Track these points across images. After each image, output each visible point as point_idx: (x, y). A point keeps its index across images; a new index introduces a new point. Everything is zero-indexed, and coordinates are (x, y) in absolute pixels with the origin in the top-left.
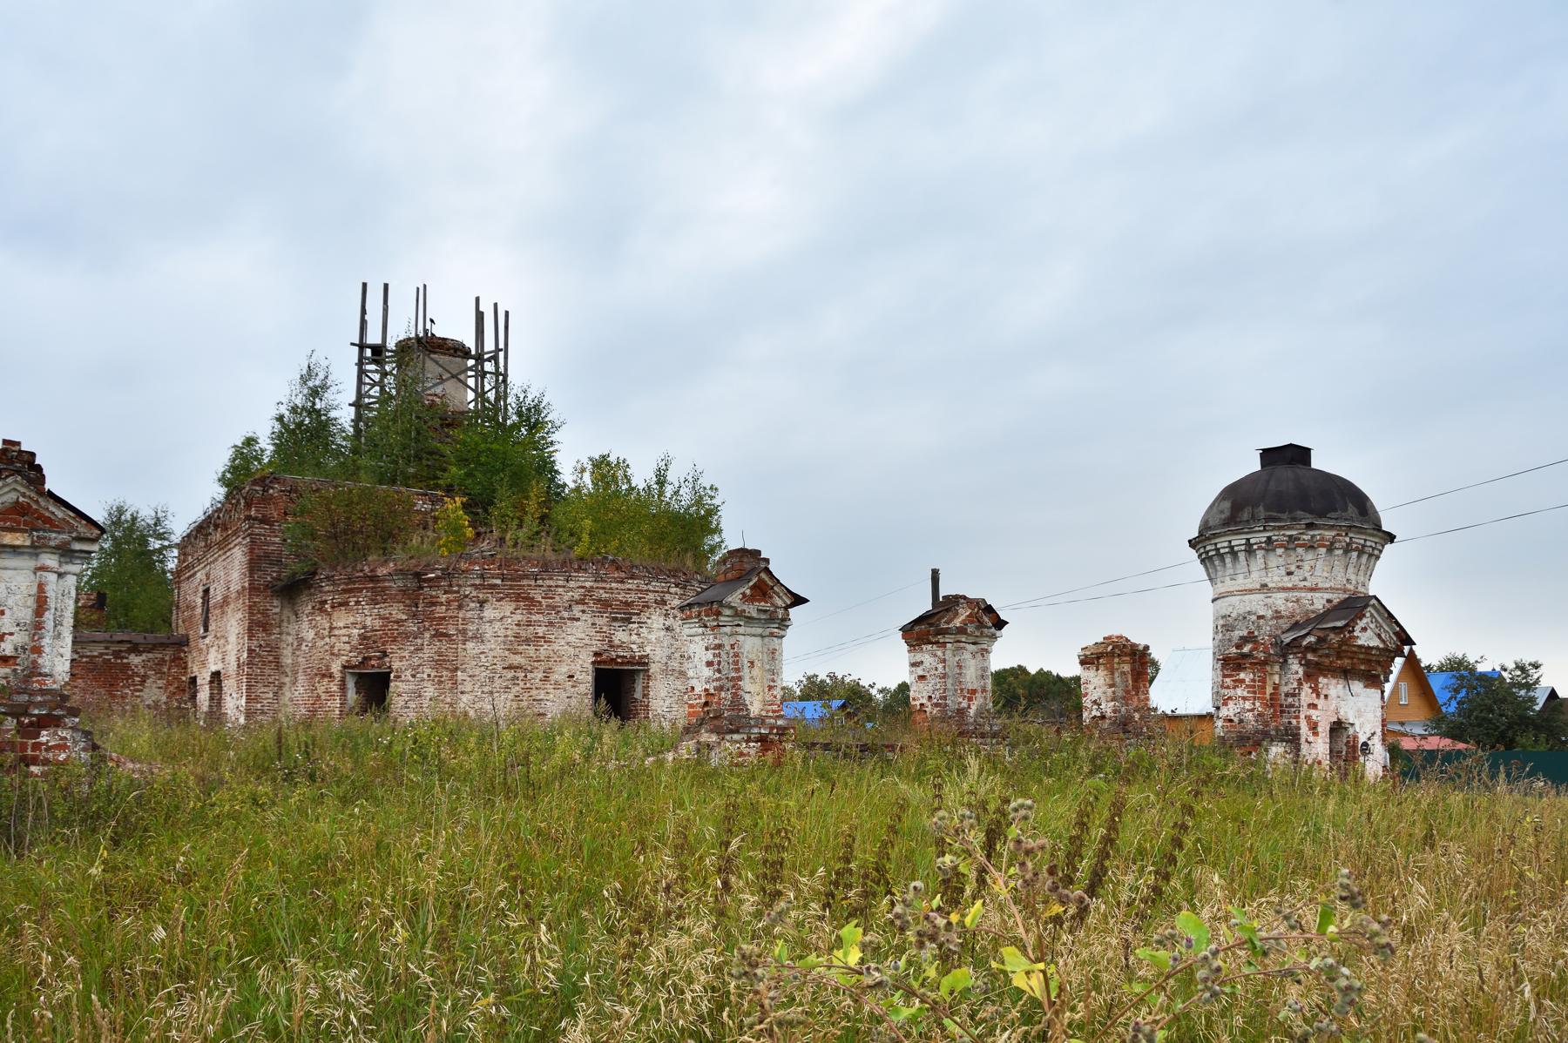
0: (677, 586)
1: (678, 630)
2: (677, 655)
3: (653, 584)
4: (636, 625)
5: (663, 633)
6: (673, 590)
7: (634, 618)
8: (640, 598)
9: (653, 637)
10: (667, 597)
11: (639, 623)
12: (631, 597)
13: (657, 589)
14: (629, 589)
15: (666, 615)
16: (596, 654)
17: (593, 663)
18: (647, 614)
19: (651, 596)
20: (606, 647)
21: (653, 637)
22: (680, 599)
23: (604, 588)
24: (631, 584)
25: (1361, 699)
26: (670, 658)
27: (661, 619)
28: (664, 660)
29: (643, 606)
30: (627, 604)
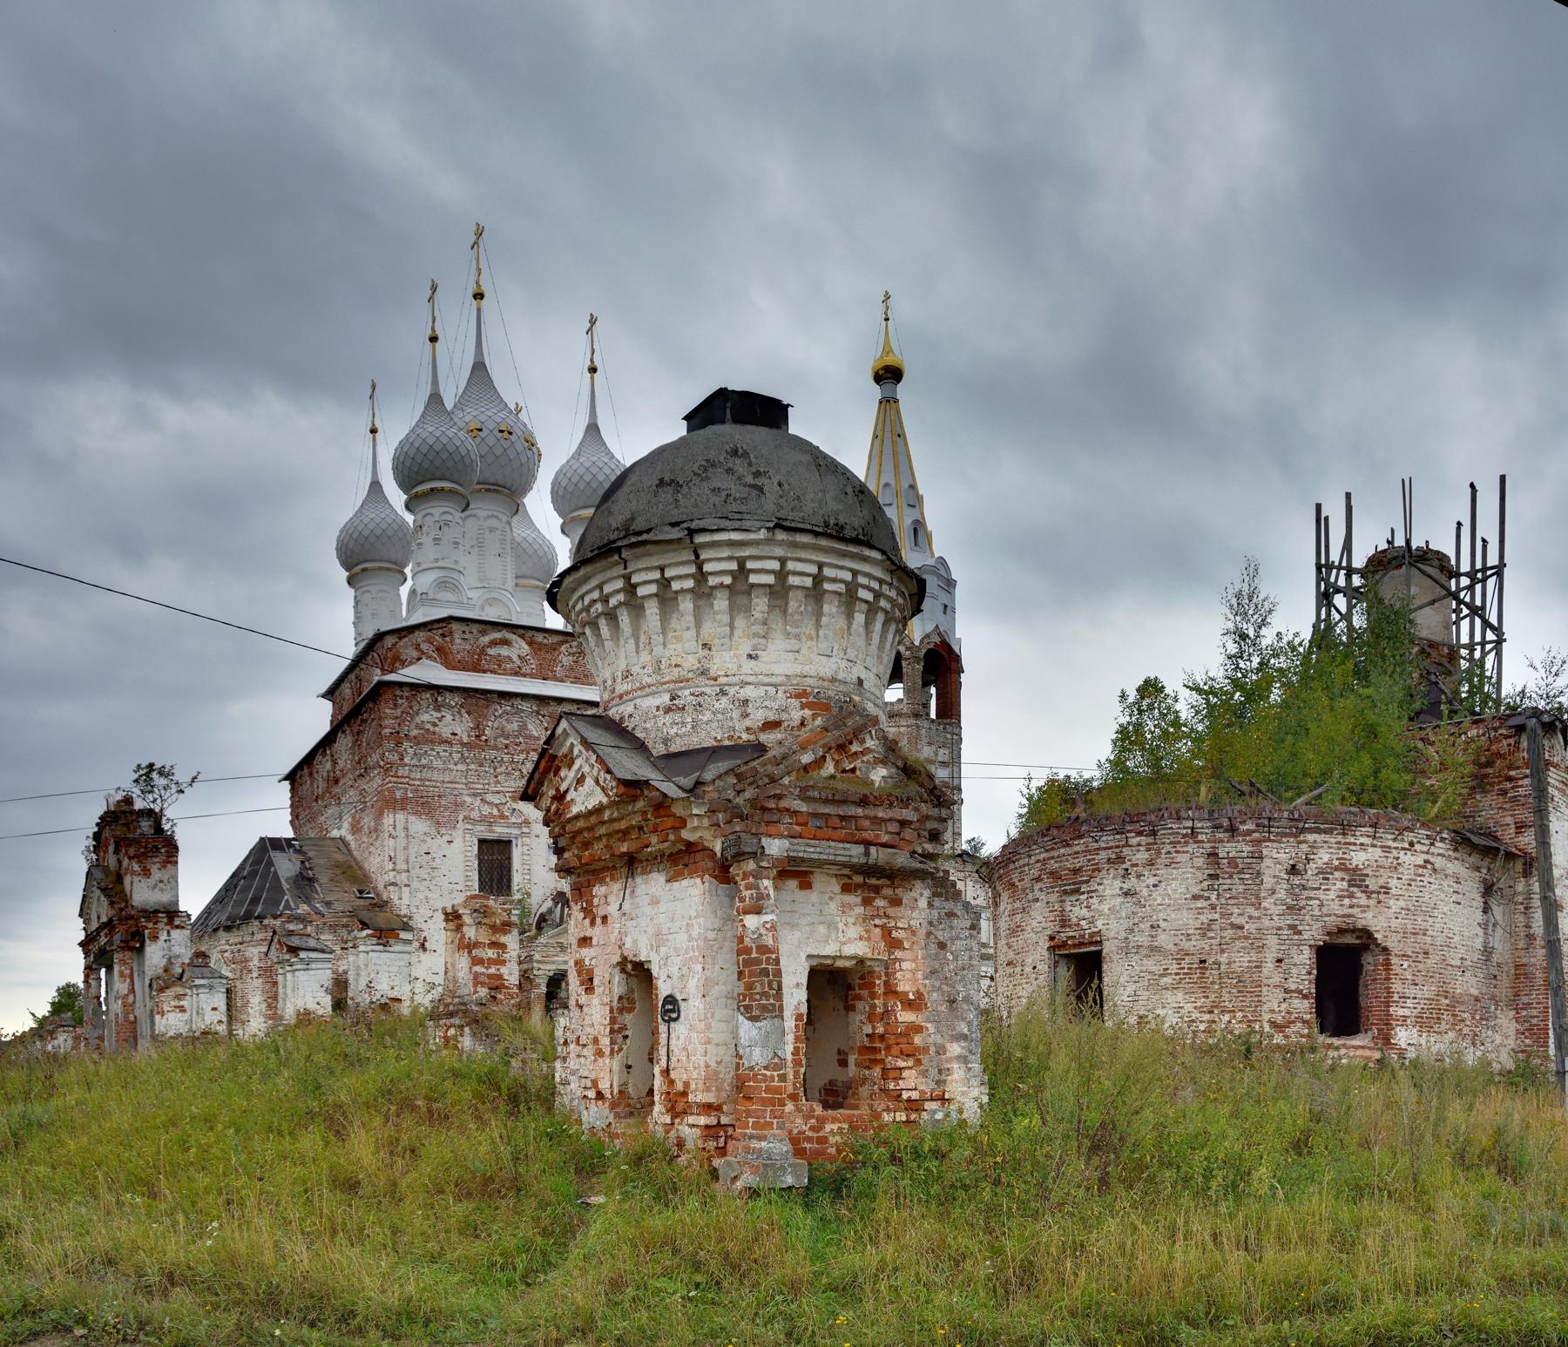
0: (1140, 834)
1: (1145, 892)
2: (1145, 926)
3: (1104, 838)
4: (1086, 896)
5: (1120, 900)
6: (1134, 841)
7: (1084, 888)
8: (1089, 861)
9: (1105, 907)
10: (1126, 851)
11: (1088, 892)
12: (1080, 862)
13: (1111, 844)
14: (1076, 853)
15: (1126, 874)
16: (1052, 938)
17: (1049, 949)
18: (1098, 880)
19: (1103, 855)
20: (1057, 929)
21: (1105, 907)
22: (1148, 850)
23: (1053, 858)
24: (1079, 846)
25: (662, 907)
26: (1132, 930)
27: (1118, 883)
28: (1123, 935)
29: (1093, 871)
30: (1076, 871)
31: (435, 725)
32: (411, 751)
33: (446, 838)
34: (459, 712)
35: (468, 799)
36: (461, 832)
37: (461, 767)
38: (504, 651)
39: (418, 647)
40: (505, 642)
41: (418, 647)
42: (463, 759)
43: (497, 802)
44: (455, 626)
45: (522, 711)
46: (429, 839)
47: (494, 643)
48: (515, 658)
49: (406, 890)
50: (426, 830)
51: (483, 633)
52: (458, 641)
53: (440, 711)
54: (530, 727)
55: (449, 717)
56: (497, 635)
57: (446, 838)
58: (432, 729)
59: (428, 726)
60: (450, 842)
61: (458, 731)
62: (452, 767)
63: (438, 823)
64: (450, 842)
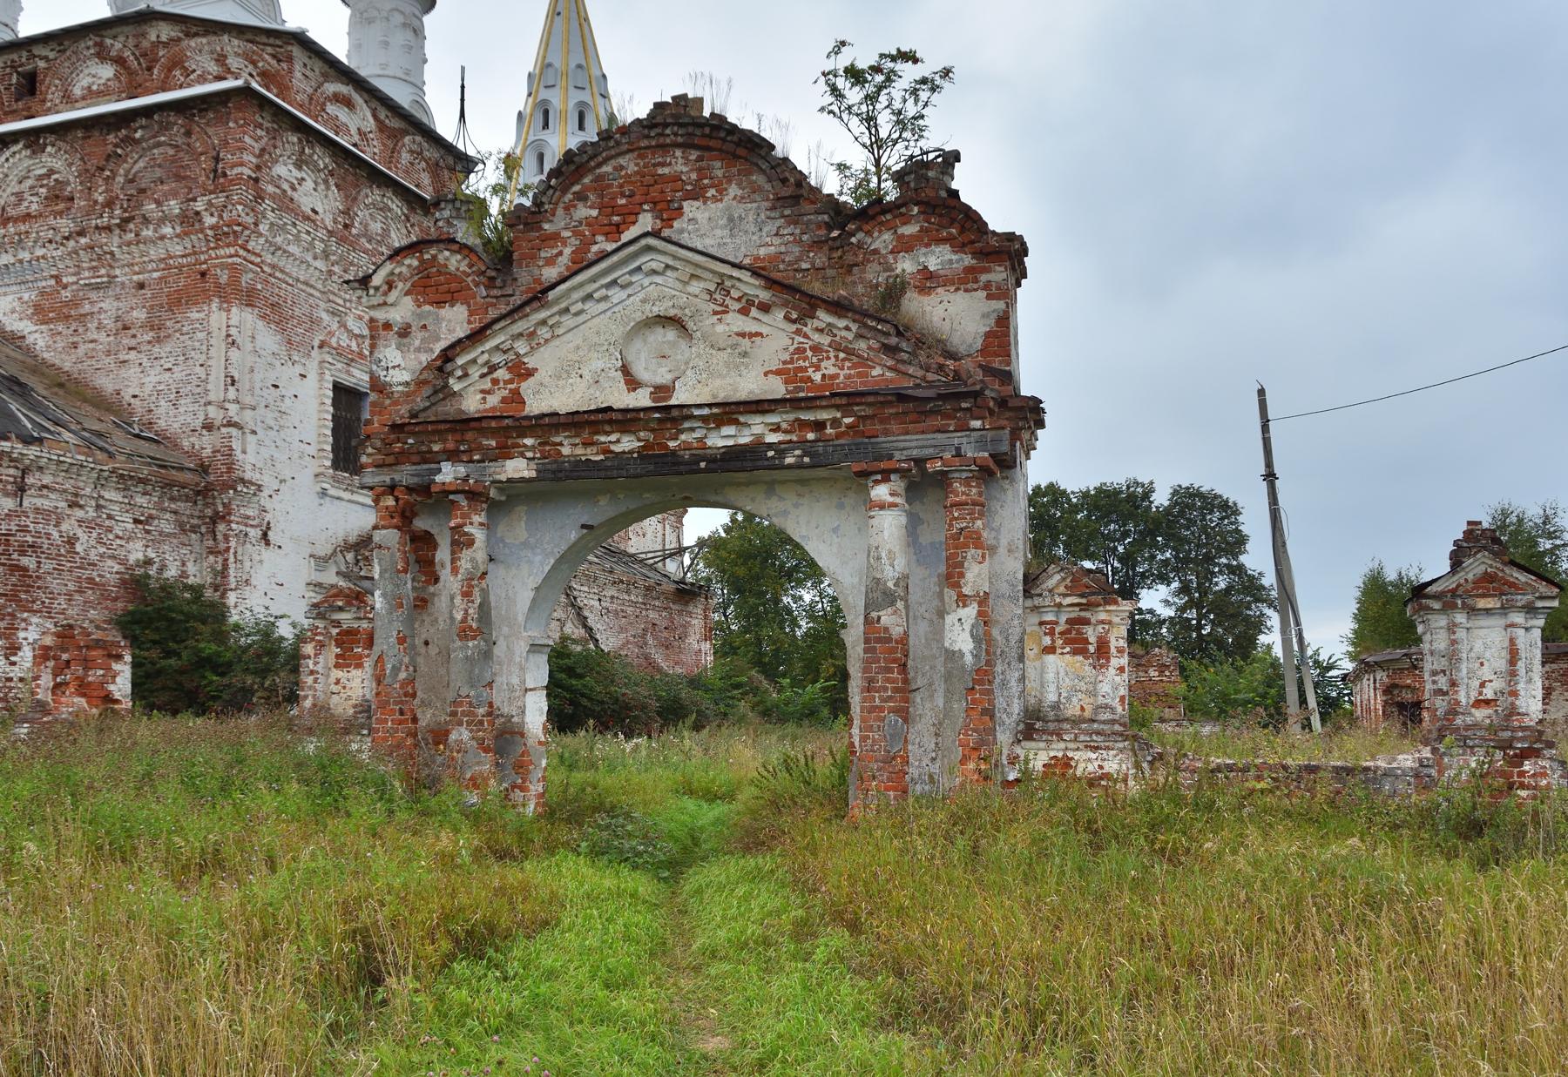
31: (294, 189)
32: (270, 214)
33: (299, 369)
34: (326, 182)
35: (324, 316)
36: (316, 363)
37: (319, 264)
38: (342, 114)
39: (221, 59)
40: (348, 103)
41: (221, 59)
42: (326, 255)
43: (357, 331)
44: (296, 51)
45: (390, 210)
46: (278, 364)
47: (337, 98)
48: (354, 131)
49: (250, 438)
50: (275, 348)
51: (326, 77)
52: (298, 75)
53: (300, 168)
54: (393, 235)
55: (309, 184)
56: (344, 89)
57: (299, 369)
58: (290, 192)
59: (286, 186)
60: (303, 376)
61: (319, 209)
62: (310, 259)
63: (289, 342)
64: (303, 376)
